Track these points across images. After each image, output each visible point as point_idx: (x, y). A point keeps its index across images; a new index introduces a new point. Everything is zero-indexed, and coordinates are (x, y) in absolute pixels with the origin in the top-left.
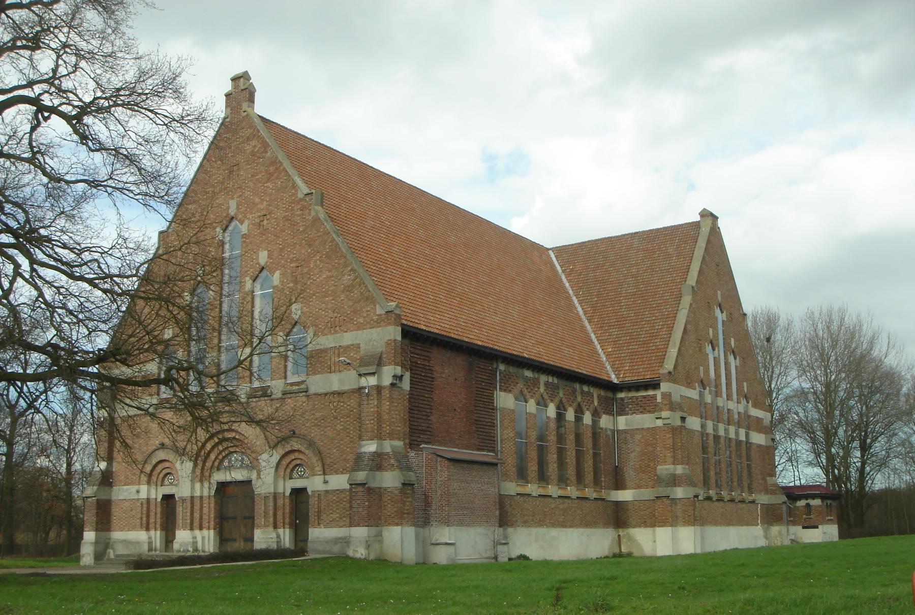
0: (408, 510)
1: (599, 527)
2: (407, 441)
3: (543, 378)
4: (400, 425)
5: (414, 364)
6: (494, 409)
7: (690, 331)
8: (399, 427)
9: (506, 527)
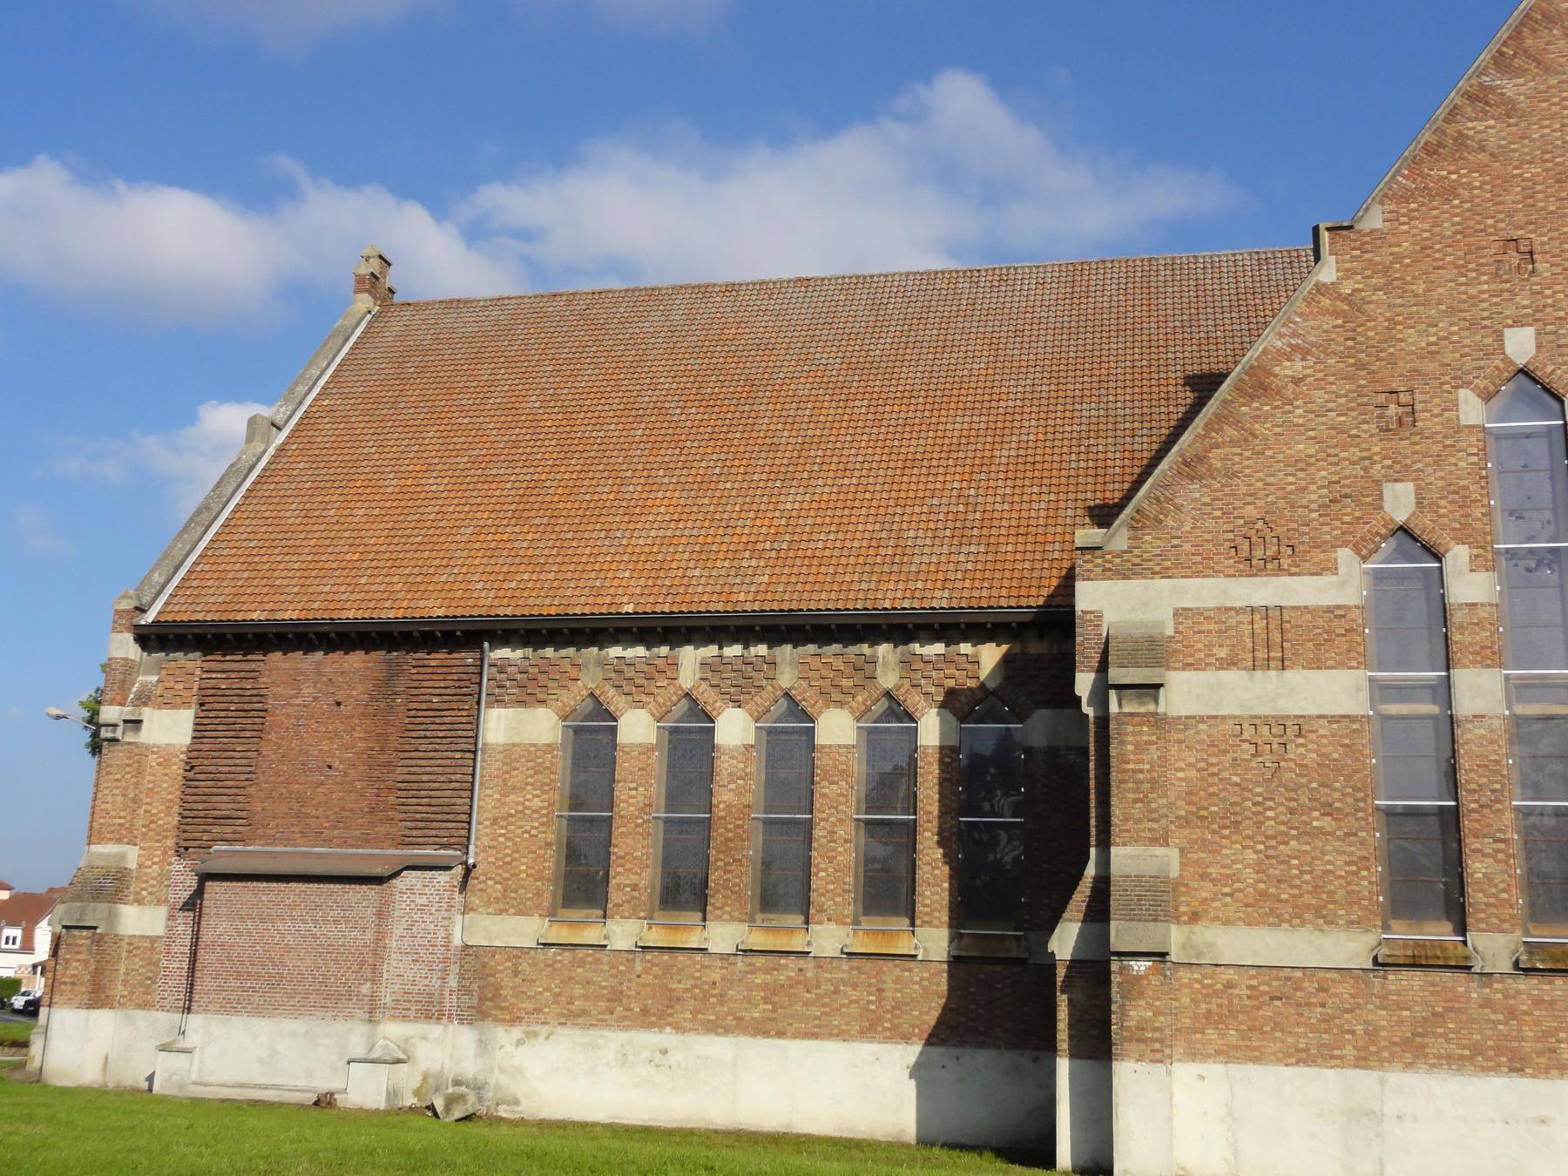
0: (73, 976)
1: (981, 1045)
2: (170, 842)
3: (691, 657)
4: (122, 814)
6: (713, 747)
7: (1297, 381)
9: (488, 1023)
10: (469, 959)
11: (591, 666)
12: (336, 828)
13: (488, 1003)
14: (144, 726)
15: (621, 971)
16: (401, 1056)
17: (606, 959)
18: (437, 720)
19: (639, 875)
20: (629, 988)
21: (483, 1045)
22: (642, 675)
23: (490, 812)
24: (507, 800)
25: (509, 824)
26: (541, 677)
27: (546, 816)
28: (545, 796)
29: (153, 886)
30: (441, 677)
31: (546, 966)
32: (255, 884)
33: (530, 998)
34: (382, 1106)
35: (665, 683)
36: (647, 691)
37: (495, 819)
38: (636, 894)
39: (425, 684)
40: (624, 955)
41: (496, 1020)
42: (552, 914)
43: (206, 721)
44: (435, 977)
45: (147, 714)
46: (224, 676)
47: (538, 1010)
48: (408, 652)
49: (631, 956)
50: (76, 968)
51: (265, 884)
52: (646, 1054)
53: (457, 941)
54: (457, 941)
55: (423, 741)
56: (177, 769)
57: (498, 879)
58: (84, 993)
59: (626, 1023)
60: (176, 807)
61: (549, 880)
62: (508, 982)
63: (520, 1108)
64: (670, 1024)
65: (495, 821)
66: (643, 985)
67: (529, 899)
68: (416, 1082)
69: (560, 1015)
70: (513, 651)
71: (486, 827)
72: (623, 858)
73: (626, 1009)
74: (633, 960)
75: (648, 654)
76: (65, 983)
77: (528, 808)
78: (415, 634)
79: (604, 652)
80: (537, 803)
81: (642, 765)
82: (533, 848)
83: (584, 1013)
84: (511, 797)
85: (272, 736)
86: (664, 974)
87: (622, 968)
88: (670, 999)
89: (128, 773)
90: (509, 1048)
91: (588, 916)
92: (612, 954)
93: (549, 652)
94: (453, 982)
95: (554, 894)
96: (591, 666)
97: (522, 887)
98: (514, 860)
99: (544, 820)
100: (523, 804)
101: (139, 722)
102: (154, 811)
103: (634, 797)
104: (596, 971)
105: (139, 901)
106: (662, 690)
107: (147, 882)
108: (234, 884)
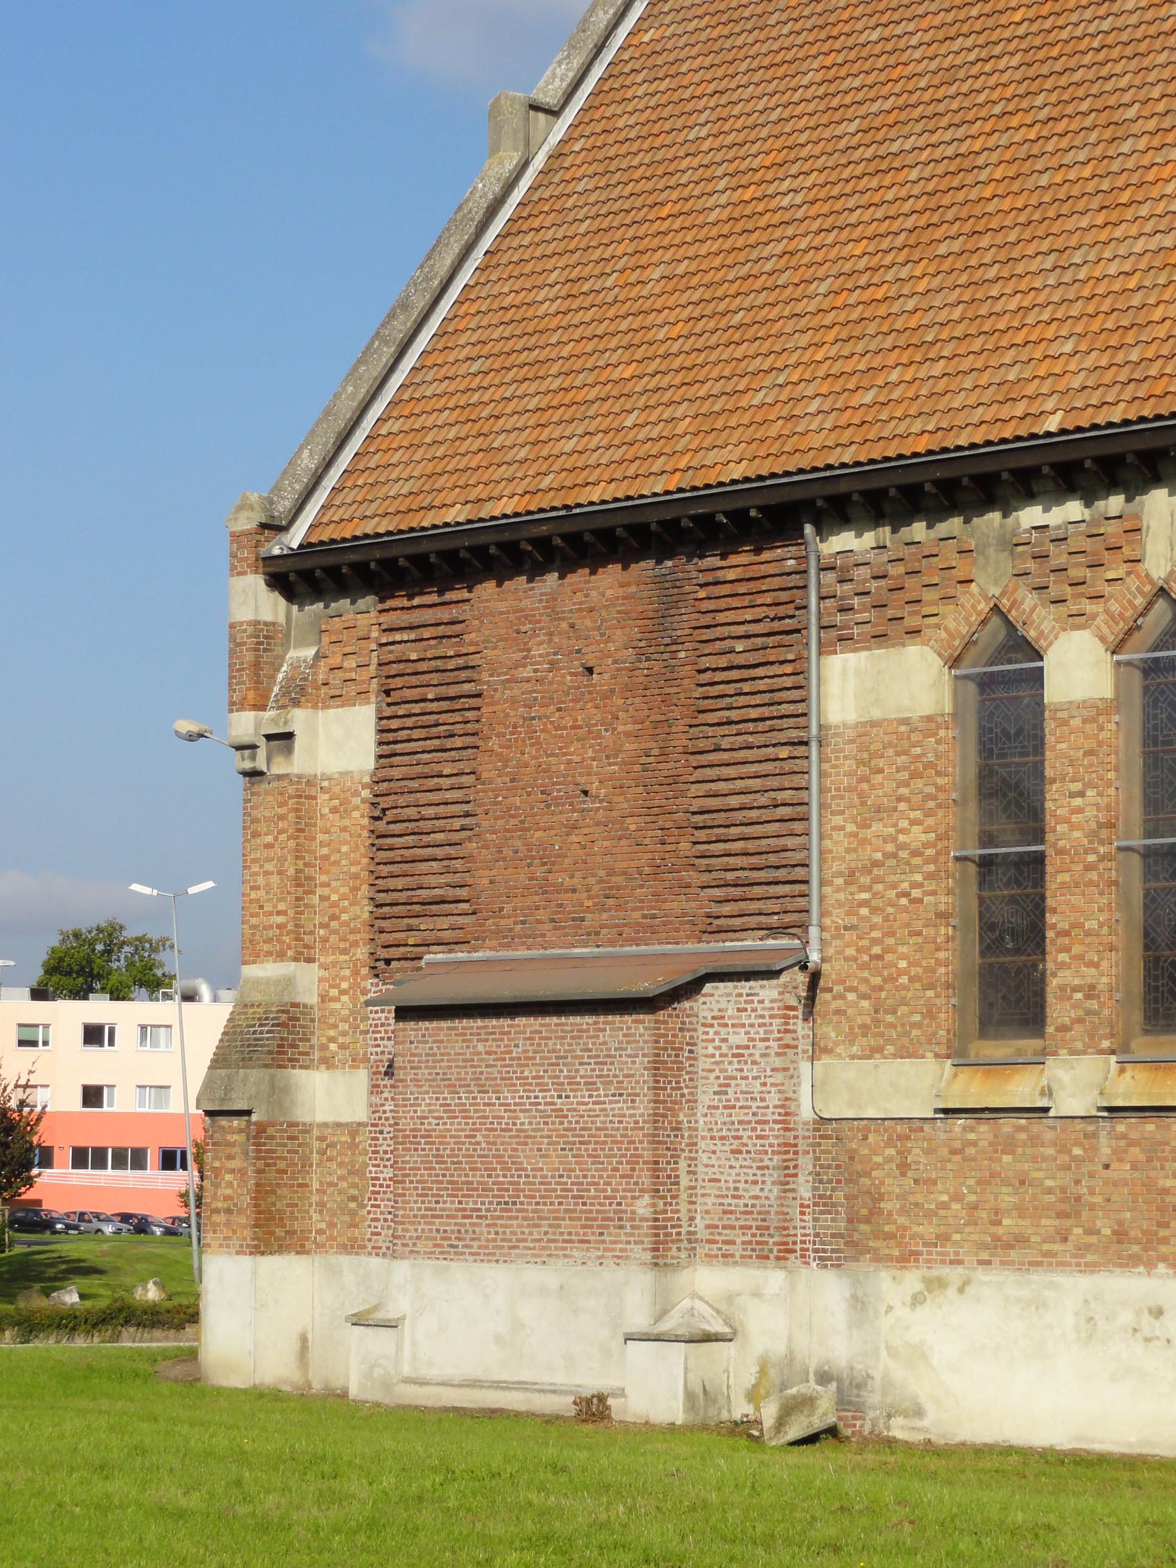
0: (227, 1198)
4: (282, 906)
5: (395, 669)
8: (279, 913)
9: (865, 1265)
10: (827, 1144)
11: (991, 551)
12: (603, 909)
13: (865, 1228)
14: (298, 742)
15: (1075, 1159)
16: (718, 1327)
17: (1049, 1135)
18: (746, 687)
19: (1096, 965)
20: (1092, 1192)
21: (859, 1305)
22: (1080, 559)
23: (843, 859)
24: (868, 833)
25: (878, 880)
26: (909, 582)
27: (934, 860)
28: (930, 821)
29: (344, 1034)
30: (746, 601)
31: (953, 1152)
32: (465, 1022)
33: (929, 1214)
34: (679, 1416)
35: (1120, 572)
36: (1092, 591)
37: (852, 873)
38: (1093, 1005)
39: (721, 618)
40: (1079, 1125)
41: (877, 1259)
42: (1121, 1049)
43: (394, 724)
44: (769, 1180)
45: (299, 719)
46: (413, 636)
47: (943, 1238)
48: (690, 559)
49: (1091, 1128)
50: (230, 1184)
51: (479, 1022)
52: (1126, 1318)
53: (806, 1113)
54: (806, 1113)
55: (725, 730)
56: (360, 818)
57: (863, 988)
58: (244, 1227)
59: (1090, 1258)
60: (365, 887)
61: (948, 986)
62: (893, 1185)
63: (925, 1423)
64: (1163, 1259)
65: (851, 877)
66: (1115, 1184)
67: (918, 1025)
68: (747, 1377)
69: (983, 1246)
70: (859, 535)
71: (838, 890)
72: (1066, 933)
73: (1089, 1232)
74: (1095, 1135)
75: (1087, 514)
76: (217, 1211)
77: (903, 846)
78: (685, 523)
79: (1010, 520)
80: (918, 836)
81: (1090, 744)
82: (917, 925)
83: (1020, 1240)
84: (876, 827)
85: (493, 743)
86: (1150, 1160)
87: (1077, 1151)
88: (1162, 1209)
89: (281, 832)
90: (902, 1311)
91: (1019, 1052)
92: (1058, 1123)
93: (918, 530)
94: (805, 1191)
95: (960, 1010)
96: (991, 551)
97: (904, 1002)
98: (888, 950)
99: (932, 868)
100: (894, 839)
101: (289, 736)
102: (334, 897)
103: (1079, 810)
104: (1034, 1159)
105: (327, 1062)
106: (1116, 588)
107: (335, 1026)
108: (435, 1024)
